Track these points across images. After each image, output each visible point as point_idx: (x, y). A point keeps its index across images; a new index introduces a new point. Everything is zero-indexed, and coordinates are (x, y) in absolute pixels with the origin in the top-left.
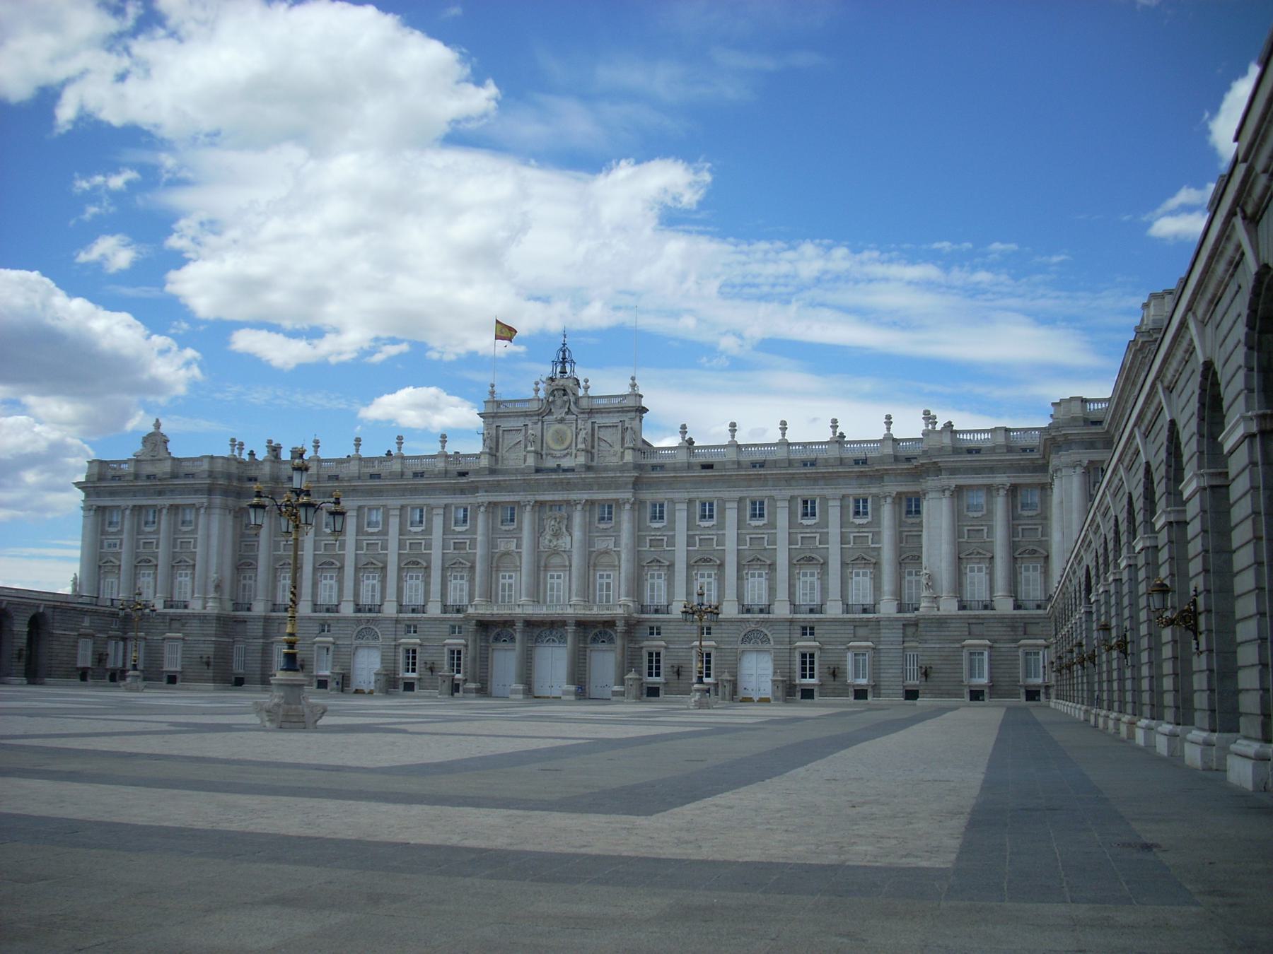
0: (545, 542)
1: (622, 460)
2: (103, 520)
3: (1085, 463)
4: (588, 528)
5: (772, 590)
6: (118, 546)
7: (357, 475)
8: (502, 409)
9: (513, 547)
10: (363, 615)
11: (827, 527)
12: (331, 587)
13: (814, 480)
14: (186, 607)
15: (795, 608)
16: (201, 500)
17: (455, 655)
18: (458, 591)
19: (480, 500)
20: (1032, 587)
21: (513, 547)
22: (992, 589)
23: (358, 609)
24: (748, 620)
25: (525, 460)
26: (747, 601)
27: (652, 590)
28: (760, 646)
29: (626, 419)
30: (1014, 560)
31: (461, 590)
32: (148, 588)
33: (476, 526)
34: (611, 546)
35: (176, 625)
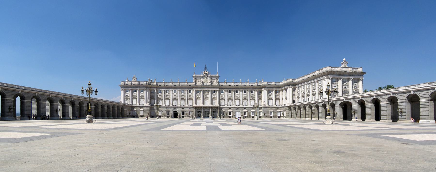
0: (205, 96)
2: (125, 91)
4: (212, 94)
5: (240, 103)
7: (172, 85)
8: (196, 76)
12: (168, 102)
13: (246, 88)
14: (143, 105)
15: (243, 106)
18: (190, 103)
21: (199, 96)
25: (201, 84)
26: (236, 104)
27: (222, 103)
31: (191, 103)
33: (193, 93)
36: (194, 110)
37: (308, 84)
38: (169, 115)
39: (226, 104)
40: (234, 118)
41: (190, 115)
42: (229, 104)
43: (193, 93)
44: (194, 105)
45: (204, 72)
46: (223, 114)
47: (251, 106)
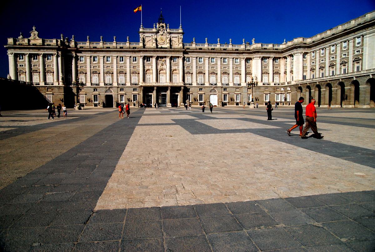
0: (159, 67)
1: (179, 46)
3: (304, 52)
5: (217, 80)
6: (24, 66)
9: (150, 68)
10: (108, 86)
11: (229, 65)
12: (96, 78)
15: (223, 84)
16: (54, 52)
17: (135, 97)
18: (135, 79)
19: (141, 55)
20: (277, 80)
21: (150, 68)
22: (268, 80)
23: (105, 84)
24: (211, 87)
25: (152, 45)
26: (211, 82)
27: (187, 79)
28: (214, 93)
29: (180, 36)
30: (273, 74)
31: (136, 79)
32: (37, 79)
34: (177, 68)
35: (49, 90)
36: (141, 94)
37: (323, 49)
38: (98, 102)
39: (193, 80)
40: (208, 106)
41: (134, 102)
42: (200, 81)
43: (138, 63)
44: (140, 84)
45: (159, 24)
46: (189, 99)
47: (234, 84)
